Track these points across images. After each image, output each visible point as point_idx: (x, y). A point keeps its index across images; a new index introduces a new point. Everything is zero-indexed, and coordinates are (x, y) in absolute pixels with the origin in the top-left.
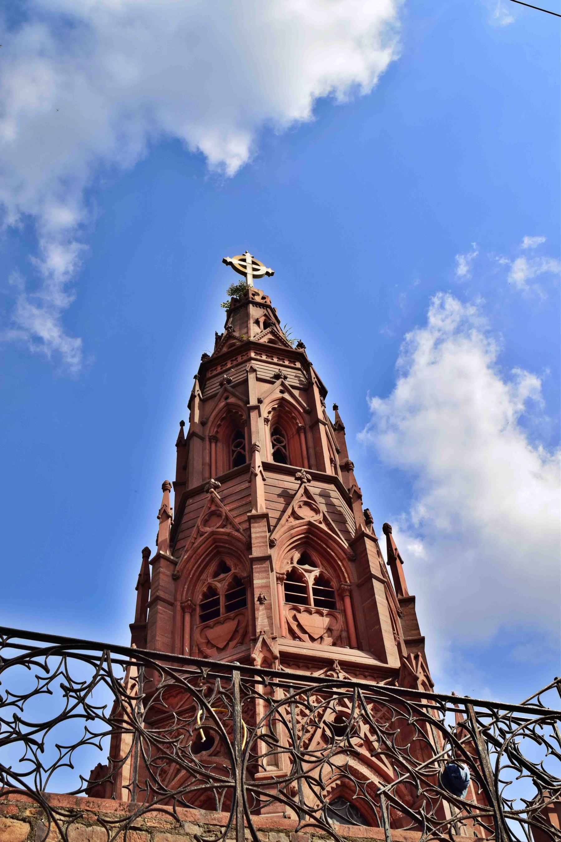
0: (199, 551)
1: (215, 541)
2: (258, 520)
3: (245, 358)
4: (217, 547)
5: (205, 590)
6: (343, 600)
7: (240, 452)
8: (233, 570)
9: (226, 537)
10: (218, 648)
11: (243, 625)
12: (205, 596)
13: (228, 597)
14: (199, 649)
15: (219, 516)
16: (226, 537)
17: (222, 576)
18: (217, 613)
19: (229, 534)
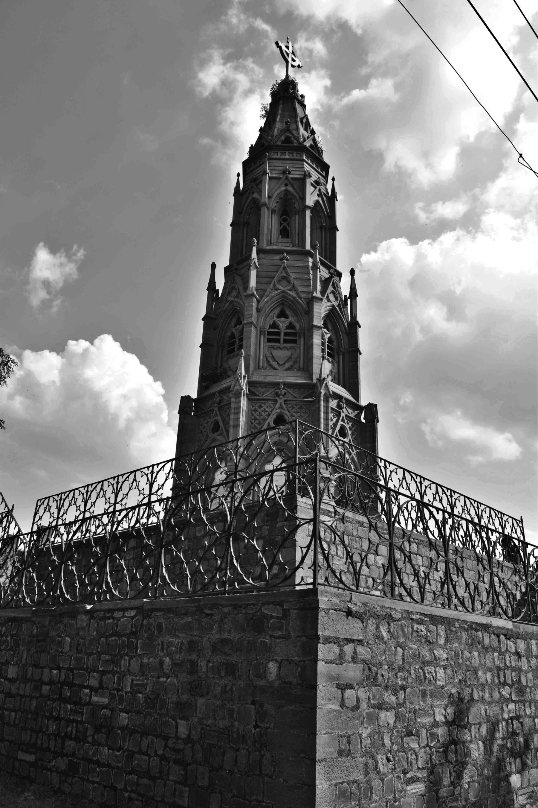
0: (274, 299)
1: (283, 296)
2: (318, 301)
3: (298, 157)
5: (272, 323)
6: (338, 355)
7: (285, 227)
8: (290, 319)
9: (292, 298)
10: (278, 364)
11: (295, 356)
13: (286, 334)
14: (267, 359)
15: (289, 282)
16: (292, 298)
17: (283, 319)
19: (294, 297)
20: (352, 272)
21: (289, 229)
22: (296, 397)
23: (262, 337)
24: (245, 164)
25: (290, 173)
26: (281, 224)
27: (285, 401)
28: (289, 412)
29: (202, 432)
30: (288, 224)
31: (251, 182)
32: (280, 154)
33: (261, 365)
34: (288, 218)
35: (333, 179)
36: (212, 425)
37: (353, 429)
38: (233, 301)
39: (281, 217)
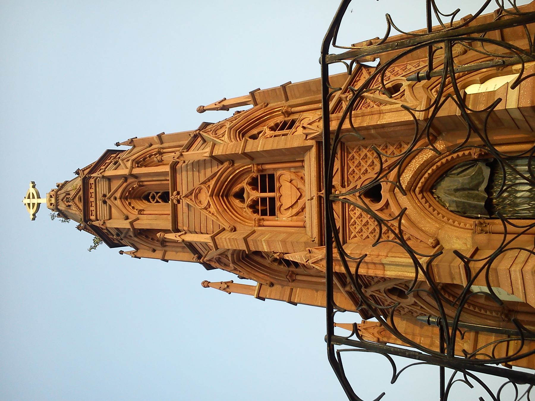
0: (220, 210)
1: (218, 195)
4: (222, 197)
7: (159, 197)
10: (299, 199)
12: (256, 211)
13: (263, 190)
17: (245, 196)
18: (272, 200)
20: (202, 110)
21: (161, 191)
22: (338, 169)
23: (266, 223)
24: (112, 245)
25: (105, 196)
26: (157, 202)
27: (343, 186)
28: (360, 178)
29: (410, 311)
30: (157, 193)
31: (122, 239)
32: (92, 208)
33: (301, 224)
34: (151, 195)
35: (118, 144)
36: (395, 298)
37: (390, 74)
38: (234, 262)
39: (150, 202)
